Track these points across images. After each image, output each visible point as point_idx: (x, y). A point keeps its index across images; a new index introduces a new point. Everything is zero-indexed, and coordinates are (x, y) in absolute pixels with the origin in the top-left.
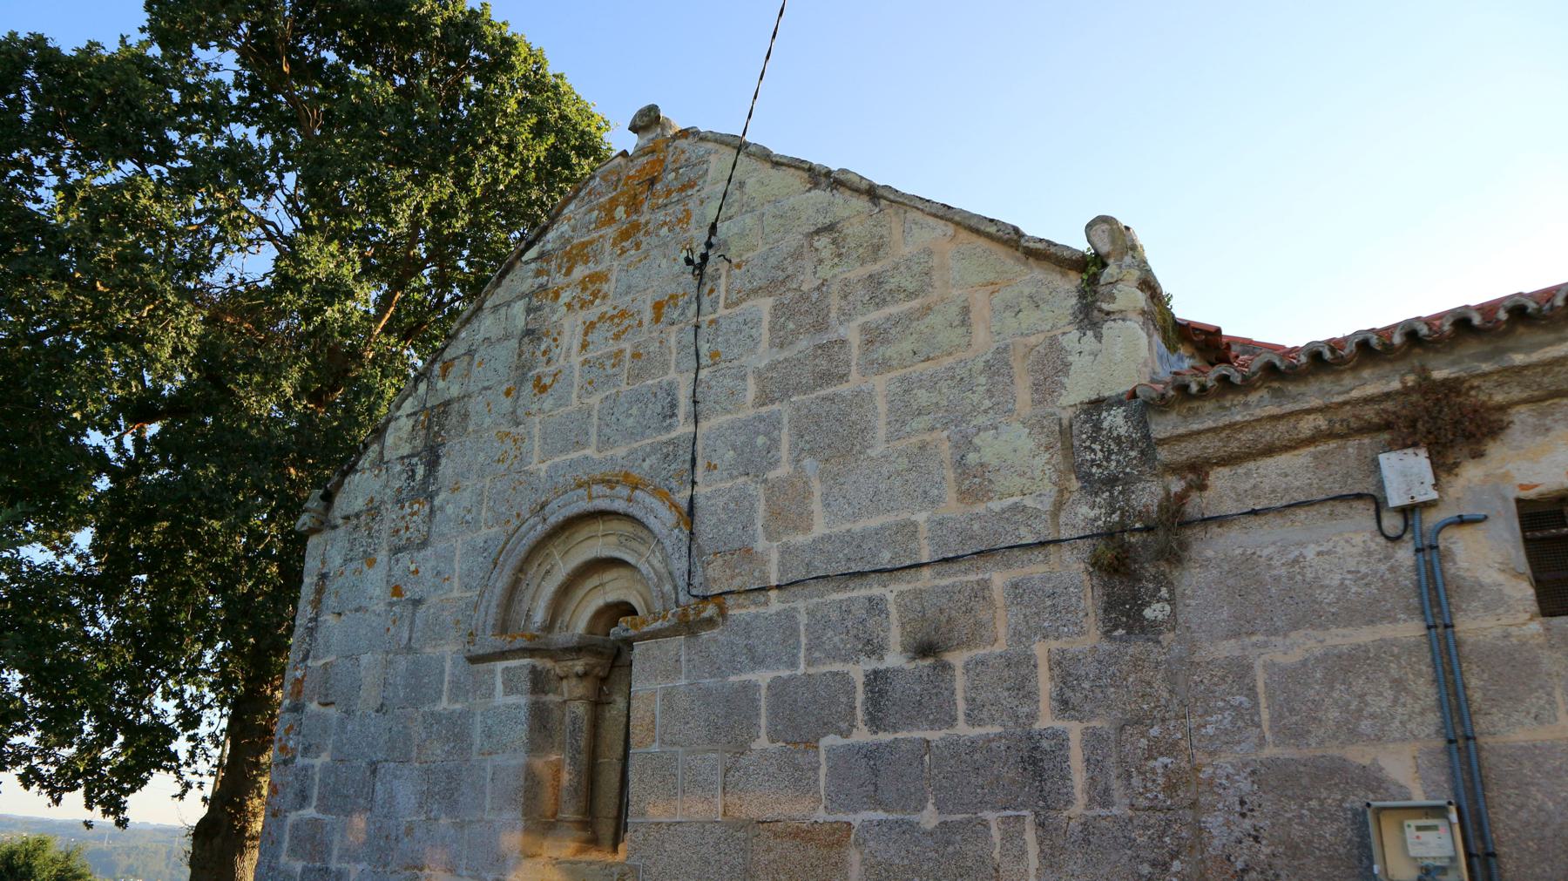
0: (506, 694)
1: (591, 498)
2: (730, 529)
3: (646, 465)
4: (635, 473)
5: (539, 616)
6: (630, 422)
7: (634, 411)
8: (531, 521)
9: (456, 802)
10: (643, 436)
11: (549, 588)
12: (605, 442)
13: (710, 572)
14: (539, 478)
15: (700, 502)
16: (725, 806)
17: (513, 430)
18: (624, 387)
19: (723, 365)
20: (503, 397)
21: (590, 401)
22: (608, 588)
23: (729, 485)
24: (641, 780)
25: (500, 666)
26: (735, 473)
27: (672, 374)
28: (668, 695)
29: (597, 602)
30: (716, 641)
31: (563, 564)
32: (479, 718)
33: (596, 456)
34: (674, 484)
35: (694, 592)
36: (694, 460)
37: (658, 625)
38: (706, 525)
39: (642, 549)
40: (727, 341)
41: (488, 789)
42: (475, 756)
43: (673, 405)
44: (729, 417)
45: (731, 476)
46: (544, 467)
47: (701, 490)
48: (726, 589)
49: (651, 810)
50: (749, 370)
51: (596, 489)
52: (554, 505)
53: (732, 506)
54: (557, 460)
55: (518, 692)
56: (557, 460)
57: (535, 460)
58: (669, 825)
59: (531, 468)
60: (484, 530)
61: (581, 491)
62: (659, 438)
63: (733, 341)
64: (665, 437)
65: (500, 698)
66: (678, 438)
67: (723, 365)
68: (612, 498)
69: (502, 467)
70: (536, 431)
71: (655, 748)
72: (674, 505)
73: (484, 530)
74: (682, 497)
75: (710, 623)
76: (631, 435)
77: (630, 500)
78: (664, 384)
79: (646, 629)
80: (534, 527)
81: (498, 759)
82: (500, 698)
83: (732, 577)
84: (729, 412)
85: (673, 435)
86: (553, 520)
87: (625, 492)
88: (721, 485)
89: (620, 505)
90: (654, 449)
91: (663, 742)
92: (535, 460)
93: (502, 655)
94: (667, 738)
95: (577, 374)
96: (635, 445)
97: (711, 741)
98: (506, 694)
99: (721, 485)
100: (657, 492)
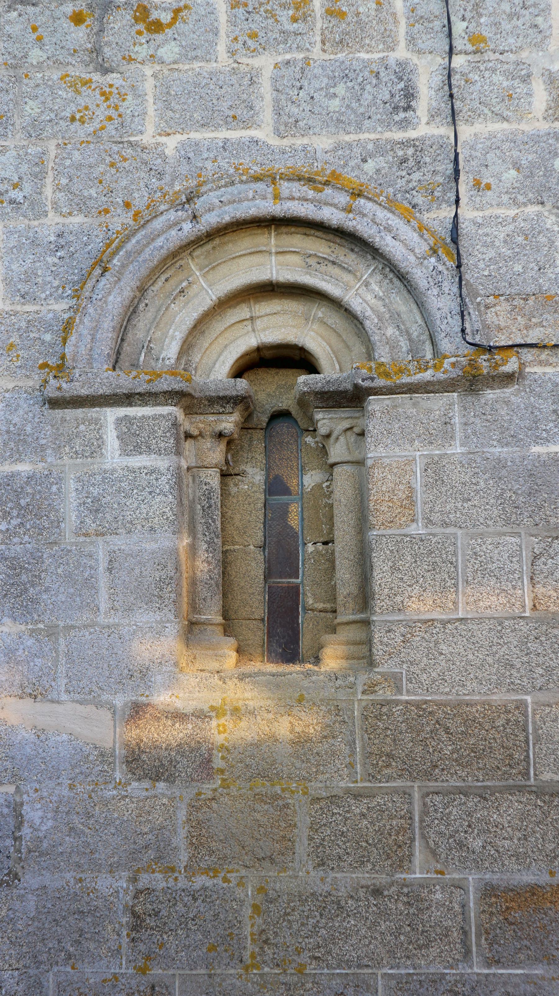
0: (125, 453)
1: (277, 197)
2: (518, 268)
3: (370, 166)
4: (351, 175)
5: (171, 351)
6: (335, 104)
7: (341, 89)
8: (172, 215)
9: (35, 601)
10: (359, 128)
11: (185, 315)
12: (287, 125)
13: (491, 317)
14: (165, 159)
15: (465, 227)
16: (536, 598)
17: (96, 77)
18: (316, 53)
19: (490, 55)
20: (67, 24)
21: (257, 62)
22: (259, 324)
23: (512, 212)
24: (394, 569)
25: (111, 414)
26: (521, 198)
27: (401, 52)
28: (434, 467)
29: (246, 342)
30: (507, 403)
31: (210, 283)
32: (72, 485)
33: (274, 142)
34: (419, 199)
35: (469, 339)
36: (457, 172)
37: (428, 375)
38: (479, 261)
39: (347, 277)
40: (497, 24)
41: (103, 581)
42: (69, 538)
43: (409, 95)
44: (505, 125)
45: (515, 203)
46: (171, 144)
47: (467, 213)
48: (519, 341)
49: (414, 605)
50: (535, 70)
51: (286, 188)
52: (212, 197)
53: (520, 239)
54: (195, 136)
55: (149, 450)
56: (195, 136)
57: (150, 129)
58: (444, 623)
59: (147, 139)
60: (53, 218)
61: (260, 186)
62: (388, 135)
63: (506, 26)
64: (399, 135)
65: (113, 455)
66: (422, 140)
67: (490, 55)
68: (319, 203)
69: (81, 131)
70: (149, 85)
71: (417, 529)
72: (421, 229)
73: (53, 218)
74: (440, 216)
75: (509, 379)
76: (339, 123)
77: (348, 210)
78: (392, 62)
79: (406, 380)
80: (176, 224)
81: (119, 542)
82: (113, 455)
83: (527, 327)
84: (506, 119)
85: (412, 134)
86: (211, 220)
87: (343, 199)
88: (501, 212)
89: (331, 215)
90: (380, 149)
91: (429, 522)
92: (150, 129)
93: (128, 399)
94: (435, 517)
95: (223, 18)
96: (347, 138)
97: (507, 522)
98: (125, 453)
99: (501, 212)
100: (391, 205)
